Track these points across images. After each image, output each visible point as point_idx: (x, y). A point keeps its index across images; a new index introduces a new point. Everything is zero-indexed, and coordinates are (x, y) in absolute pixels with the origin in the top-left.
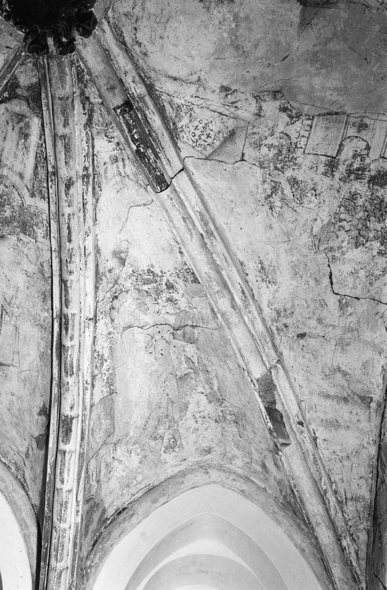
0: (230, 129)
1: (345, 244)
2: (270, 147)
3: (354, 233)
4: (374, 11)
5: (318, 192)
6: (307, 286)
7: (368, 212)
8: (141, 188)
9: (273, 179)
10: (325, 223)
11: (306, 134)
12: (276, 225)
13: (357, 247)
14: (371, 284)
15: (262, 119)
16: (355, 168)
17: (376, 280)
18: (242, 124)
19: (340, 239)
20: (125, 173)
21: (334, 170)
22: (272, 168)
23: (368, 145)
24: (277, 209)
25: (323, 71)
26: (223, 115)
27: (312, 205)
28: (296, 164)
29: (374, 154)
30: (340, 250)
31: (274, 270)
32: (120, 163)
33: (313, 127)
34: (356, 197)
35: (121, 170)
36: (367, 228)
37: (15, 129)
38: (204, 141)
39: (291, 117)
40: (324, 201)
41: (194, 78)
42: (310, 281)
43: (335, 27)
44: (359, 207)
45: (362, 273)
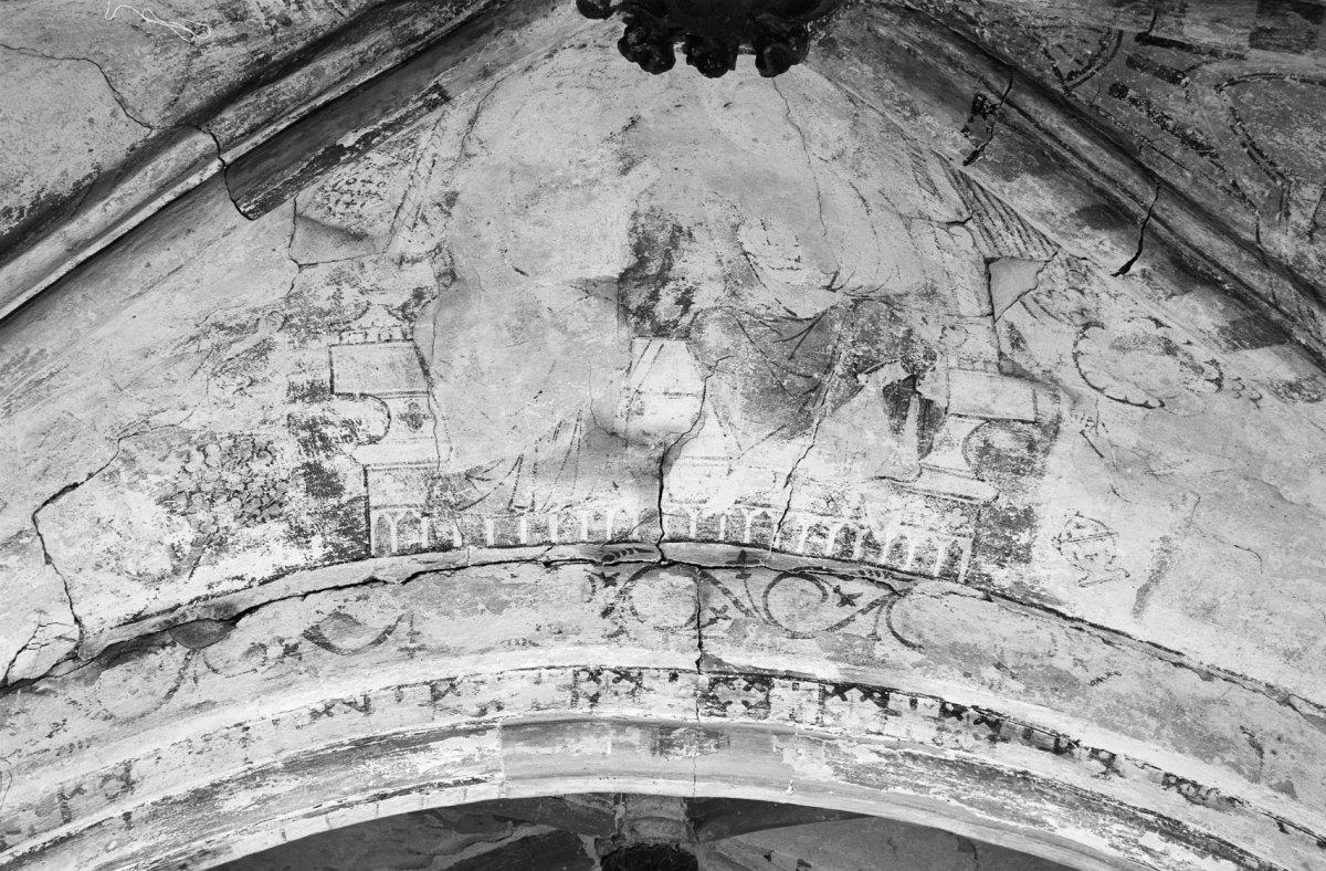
0: (369, 231)
1: (158, 479)
2: (337, 297)
3: (188, 484)
4: (624, 384)
5: (249, 390)
6: (23, 463)
7: (246, 489)
8: (173, 90)
9: (261, 324)
10: (185, 425)
11: (369, 339)
12: (153, 359)
13: (160, 502)
14: (98, 566)
15: (394, 268)
16: (324, 431)
17: (112, 570)
18: (381, 245)
19: (162, 466)
20: (205, 46)
21: (307, 399)
22: (288, 312)
23: (379, 439)
24: (194, 348)
25: (505, 334)
26: (398, 211)
27: (217, 392)
28: (304, 341)
29: (366, 454)
30: (136, 478)
31: (40, 398)
32: (229, 31)
33: (389, 344)
35: (210, 34)
36: (212, 501)
39: (404, 307)
40: (232, 407)
41: (473, 148)
42: (39, 462)
43: (586, 332)
45: (110, 539)
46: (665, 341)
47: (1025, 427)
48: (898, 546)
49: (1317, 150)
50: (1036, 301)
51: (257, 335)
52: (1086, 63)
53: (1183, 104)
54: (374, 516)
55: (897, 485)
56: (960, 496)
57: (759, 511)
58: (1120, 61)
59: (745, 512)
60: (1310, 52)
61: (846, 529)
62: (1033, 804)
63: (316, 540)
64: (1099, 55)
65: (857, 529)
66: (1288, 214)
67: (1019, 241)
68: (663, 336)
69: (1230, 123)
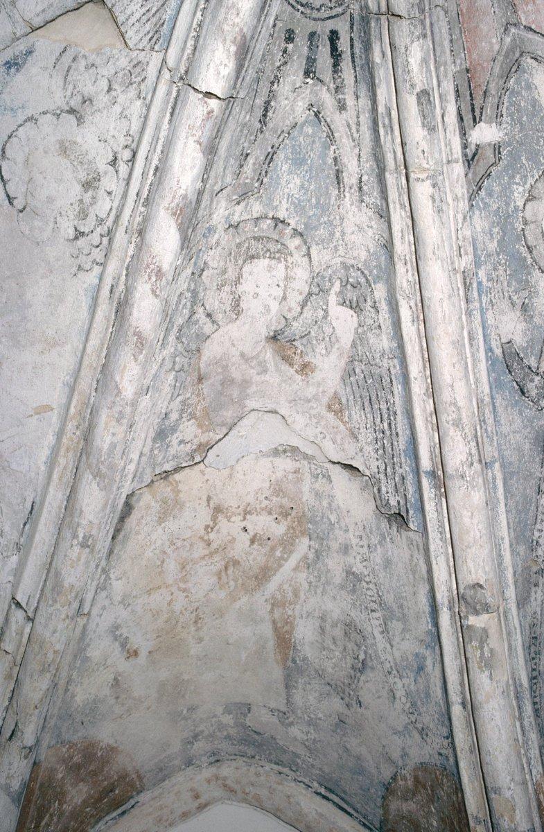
49: (286, 196)
50: (74, 59)
53: (291, 89)
58: (311, 26)
60: (426, 133)
64: (312, 9)
66: (238, 203)
67: (137, 15)
69: (285, 129)
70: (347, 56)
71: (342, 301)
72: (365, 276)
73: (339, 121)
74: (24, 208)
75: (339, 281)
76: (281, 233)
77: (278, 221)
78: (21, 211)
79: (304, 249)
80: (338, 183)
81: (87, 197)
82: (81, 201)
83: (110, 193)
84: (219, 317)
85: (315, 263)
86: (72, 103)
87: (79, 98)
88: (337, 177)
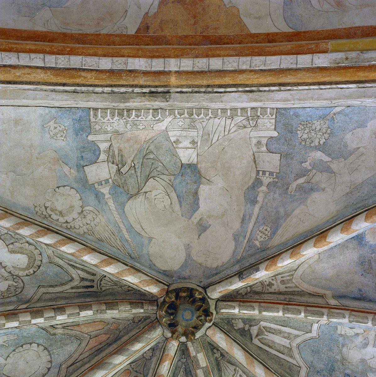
25: (232, 169)
34: (303, 138)
37: (266, 334)
38: (269, 232)
44: (309, 136)
46: (188, 163)
47: (85, 164)
48: (113, 115)
50: (96, 214)
51: (297, 183)
52: (103, 279)
54: (274, 117)
55: (117, 133)
56: (97, 134)
57: (157, 119)
59: (161, 118)
61: (129, 118)
62: (59, 81)
63: (291, 113)
65: (126, 118)
68: (189, 165)
70: (86, 290)
71: (10, 285)
72: (19, 294)
73: (68, 287)
74: (56, 191)
75: (17, 285)
76: (35, 267)
77: (39, 267)
78: (55, 190)
79: (29, 274)
80: (49, 286)
81: (57, 212)
82: (56, 210)
83: (58, 220)
84: (11, 246)
85: (24, 278)
86: (84, 212)
87: (86, 214)
88: (51, 286)
